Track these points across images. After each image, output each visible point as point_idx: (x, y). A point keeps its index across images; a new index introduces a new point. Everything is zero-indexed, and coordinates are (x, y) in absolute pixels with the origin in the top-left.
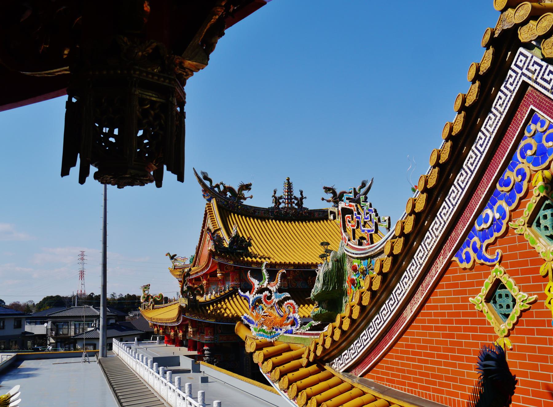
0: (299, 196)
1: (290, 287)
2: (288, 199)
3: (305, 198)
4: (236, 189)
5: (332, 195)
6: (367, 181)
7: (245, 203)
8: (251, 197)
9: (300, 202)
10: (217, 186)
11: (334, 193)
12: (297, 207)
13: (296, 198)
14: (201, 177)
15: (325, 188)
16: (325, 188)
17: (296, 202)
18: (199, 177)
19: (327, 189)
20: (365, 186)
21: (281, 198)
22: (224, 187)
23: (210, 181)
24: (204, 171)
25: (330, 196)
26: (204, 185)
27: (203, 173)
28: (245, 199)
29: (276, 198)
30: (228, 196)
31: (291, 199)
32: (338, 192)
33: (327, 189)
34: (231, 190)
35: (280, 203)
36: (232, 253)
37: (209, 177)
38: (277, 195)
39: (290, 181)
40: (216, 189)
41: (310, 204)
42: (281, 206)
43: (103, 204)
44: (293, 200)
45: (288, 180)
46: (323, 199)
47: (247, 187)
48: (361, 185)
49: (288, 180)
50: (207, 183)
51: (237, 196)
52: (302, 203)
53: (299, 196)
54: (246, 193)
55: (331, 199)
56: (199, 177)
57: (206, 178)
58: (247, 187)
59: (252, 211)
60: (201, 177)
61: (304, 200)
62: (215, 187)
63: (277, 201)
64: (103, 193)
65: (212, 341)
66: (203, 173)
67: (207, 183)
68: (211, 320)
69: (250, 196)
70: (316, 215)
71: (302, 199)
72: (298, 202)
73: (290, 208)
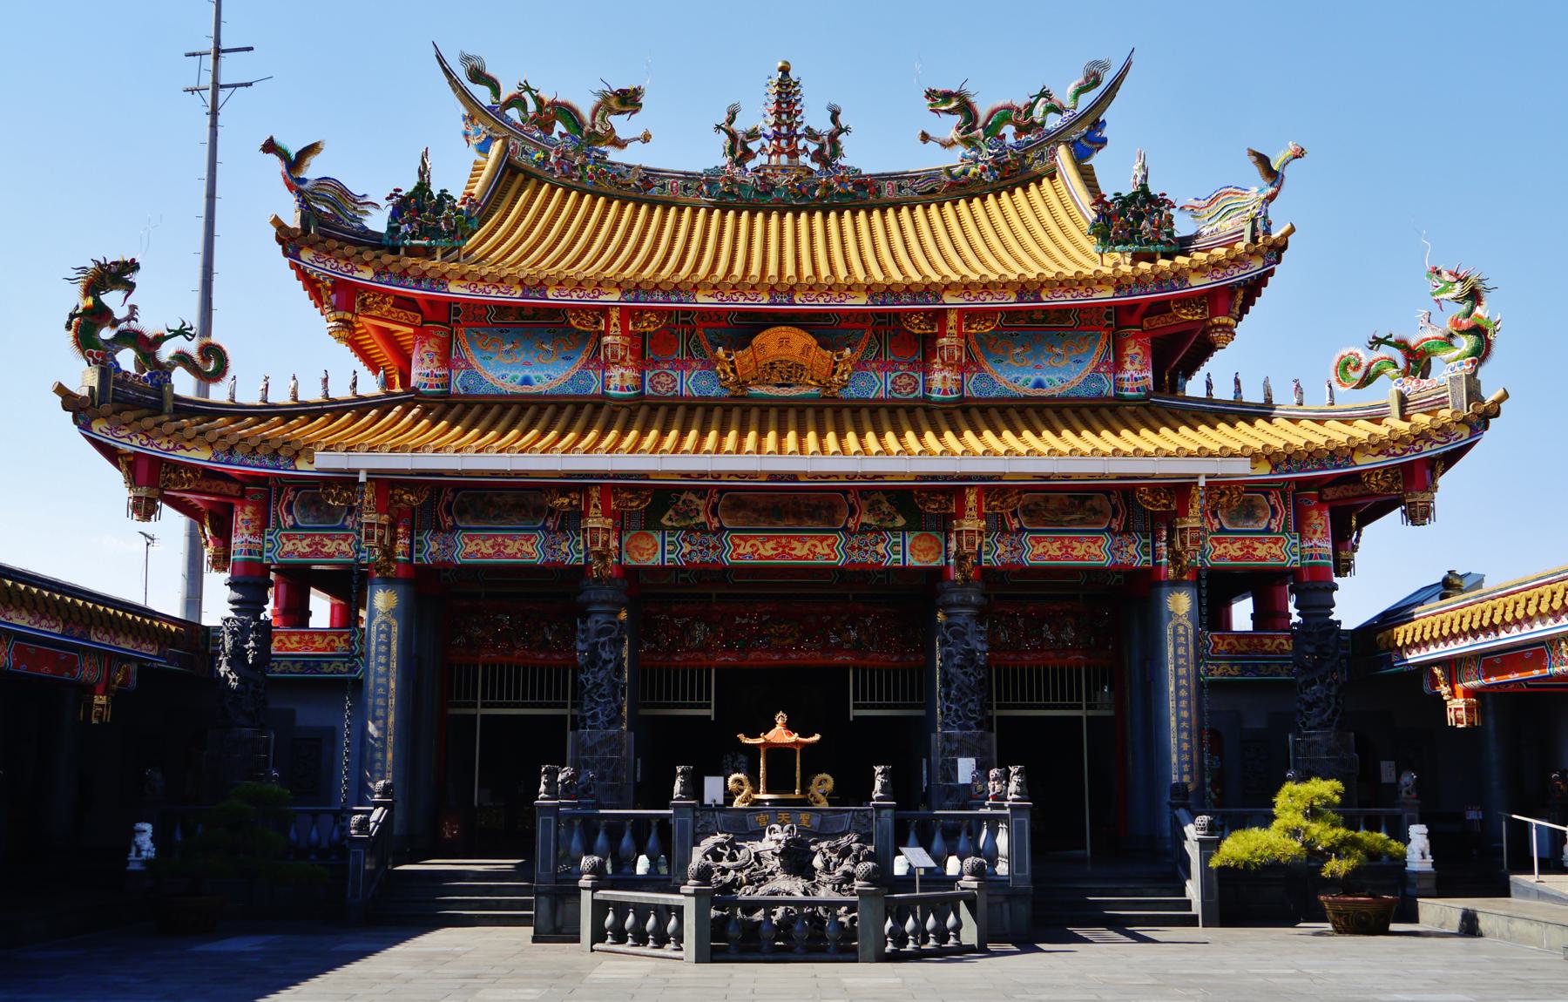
0: (824, 126)
1: (648, 390)
2: (777, 136)
3: (846, 130)
4: (585, 109)
5: (958, 119)
6: (1106, 67)
7: (614, 155)
8: (646, 138)
9: (829, 150)
10: (517, 101)
11: (966, 108)
12: (816, 167)
13: (811, 134)
14: (461, 73)
15: (931, 94)
16: (931, 94)
17: (813, 147)
18: (448, 73)
19: (938, 98)
20: (1097, 83)
21: (753, 135)
22: (539, 101)
23: (495, 87)
24: (470, 52)
25: (948, 126)
26: (466, 97)
27: (466, 59)
28: (621, 144)
29: (733, 136)
30: (555, 135)
31: (791, 136)
32: (983, 111)
33: (938, 98)
34: (567, 112)
35: (749, 154)
36: (394, 250)
37: (490, 71)
38: (740, 126)
39: (793, 75)
40: (514, 114)
41: (864, 155)
42: (750, 165)
43: (202, 211)
44: (801, 144)
45: (785, 70)
46: (925, 137)
47: (628, 100)
48: (1081, 79)
49: (785, 70)
50: (482, 94)
51: (592, 138)
52: (836, 151)
53: (824, 126)
54: (622, 125)
55: (953, 134)
56: (448, 73)
57: (478, 75)
58: (628, 100)
59: (634, 181)
60: (461, 73)
61: (841, 137)
62: (510, 103)
63: (739, 148)
64: (205, 174)
65: (250, 552)
66: (466, 59)
67: (482, 94)
68: (194, 454)
69: (640, 134)
70: (888, 191)
71: (833, 138)
72: (822, 146)
73: (784, 170)
